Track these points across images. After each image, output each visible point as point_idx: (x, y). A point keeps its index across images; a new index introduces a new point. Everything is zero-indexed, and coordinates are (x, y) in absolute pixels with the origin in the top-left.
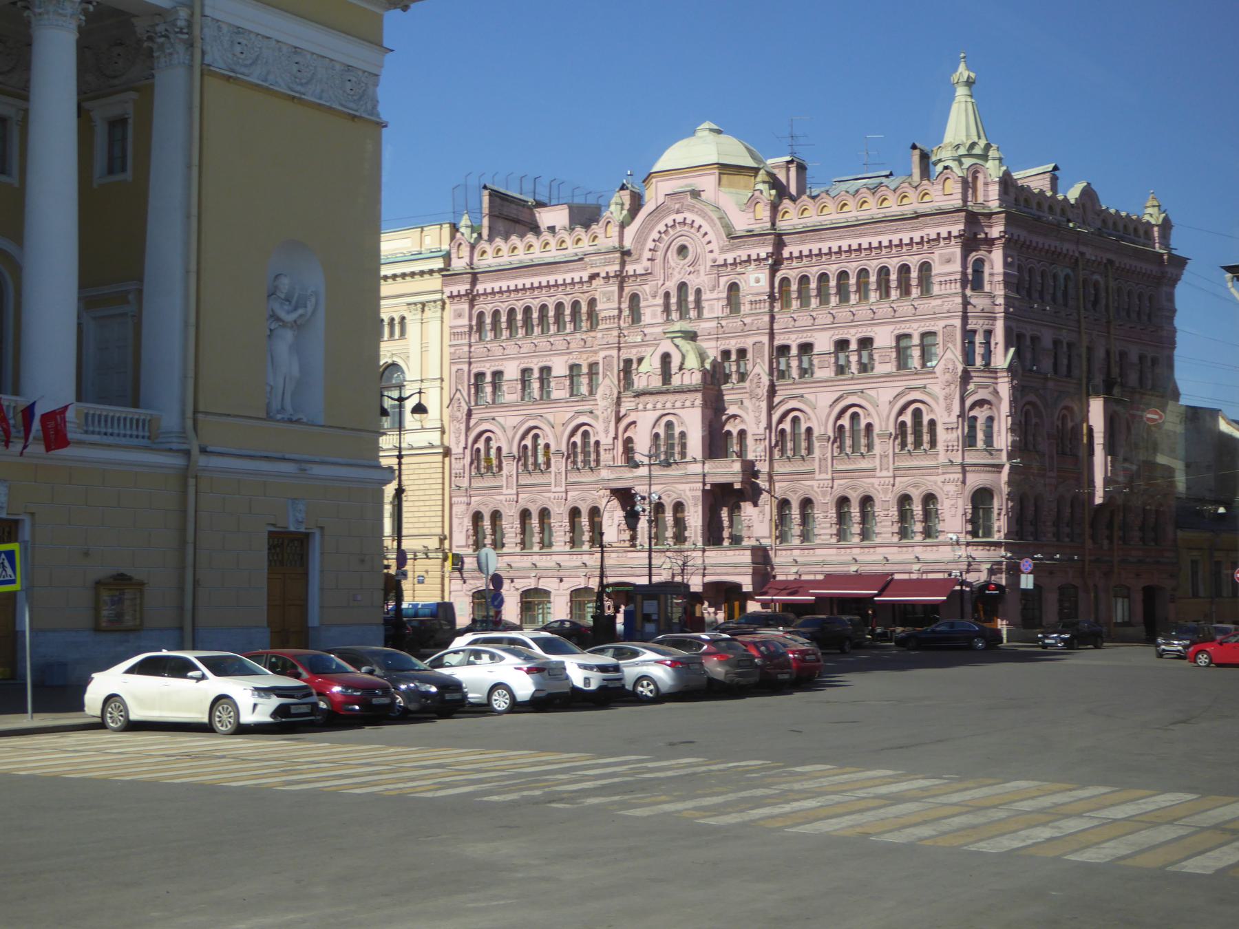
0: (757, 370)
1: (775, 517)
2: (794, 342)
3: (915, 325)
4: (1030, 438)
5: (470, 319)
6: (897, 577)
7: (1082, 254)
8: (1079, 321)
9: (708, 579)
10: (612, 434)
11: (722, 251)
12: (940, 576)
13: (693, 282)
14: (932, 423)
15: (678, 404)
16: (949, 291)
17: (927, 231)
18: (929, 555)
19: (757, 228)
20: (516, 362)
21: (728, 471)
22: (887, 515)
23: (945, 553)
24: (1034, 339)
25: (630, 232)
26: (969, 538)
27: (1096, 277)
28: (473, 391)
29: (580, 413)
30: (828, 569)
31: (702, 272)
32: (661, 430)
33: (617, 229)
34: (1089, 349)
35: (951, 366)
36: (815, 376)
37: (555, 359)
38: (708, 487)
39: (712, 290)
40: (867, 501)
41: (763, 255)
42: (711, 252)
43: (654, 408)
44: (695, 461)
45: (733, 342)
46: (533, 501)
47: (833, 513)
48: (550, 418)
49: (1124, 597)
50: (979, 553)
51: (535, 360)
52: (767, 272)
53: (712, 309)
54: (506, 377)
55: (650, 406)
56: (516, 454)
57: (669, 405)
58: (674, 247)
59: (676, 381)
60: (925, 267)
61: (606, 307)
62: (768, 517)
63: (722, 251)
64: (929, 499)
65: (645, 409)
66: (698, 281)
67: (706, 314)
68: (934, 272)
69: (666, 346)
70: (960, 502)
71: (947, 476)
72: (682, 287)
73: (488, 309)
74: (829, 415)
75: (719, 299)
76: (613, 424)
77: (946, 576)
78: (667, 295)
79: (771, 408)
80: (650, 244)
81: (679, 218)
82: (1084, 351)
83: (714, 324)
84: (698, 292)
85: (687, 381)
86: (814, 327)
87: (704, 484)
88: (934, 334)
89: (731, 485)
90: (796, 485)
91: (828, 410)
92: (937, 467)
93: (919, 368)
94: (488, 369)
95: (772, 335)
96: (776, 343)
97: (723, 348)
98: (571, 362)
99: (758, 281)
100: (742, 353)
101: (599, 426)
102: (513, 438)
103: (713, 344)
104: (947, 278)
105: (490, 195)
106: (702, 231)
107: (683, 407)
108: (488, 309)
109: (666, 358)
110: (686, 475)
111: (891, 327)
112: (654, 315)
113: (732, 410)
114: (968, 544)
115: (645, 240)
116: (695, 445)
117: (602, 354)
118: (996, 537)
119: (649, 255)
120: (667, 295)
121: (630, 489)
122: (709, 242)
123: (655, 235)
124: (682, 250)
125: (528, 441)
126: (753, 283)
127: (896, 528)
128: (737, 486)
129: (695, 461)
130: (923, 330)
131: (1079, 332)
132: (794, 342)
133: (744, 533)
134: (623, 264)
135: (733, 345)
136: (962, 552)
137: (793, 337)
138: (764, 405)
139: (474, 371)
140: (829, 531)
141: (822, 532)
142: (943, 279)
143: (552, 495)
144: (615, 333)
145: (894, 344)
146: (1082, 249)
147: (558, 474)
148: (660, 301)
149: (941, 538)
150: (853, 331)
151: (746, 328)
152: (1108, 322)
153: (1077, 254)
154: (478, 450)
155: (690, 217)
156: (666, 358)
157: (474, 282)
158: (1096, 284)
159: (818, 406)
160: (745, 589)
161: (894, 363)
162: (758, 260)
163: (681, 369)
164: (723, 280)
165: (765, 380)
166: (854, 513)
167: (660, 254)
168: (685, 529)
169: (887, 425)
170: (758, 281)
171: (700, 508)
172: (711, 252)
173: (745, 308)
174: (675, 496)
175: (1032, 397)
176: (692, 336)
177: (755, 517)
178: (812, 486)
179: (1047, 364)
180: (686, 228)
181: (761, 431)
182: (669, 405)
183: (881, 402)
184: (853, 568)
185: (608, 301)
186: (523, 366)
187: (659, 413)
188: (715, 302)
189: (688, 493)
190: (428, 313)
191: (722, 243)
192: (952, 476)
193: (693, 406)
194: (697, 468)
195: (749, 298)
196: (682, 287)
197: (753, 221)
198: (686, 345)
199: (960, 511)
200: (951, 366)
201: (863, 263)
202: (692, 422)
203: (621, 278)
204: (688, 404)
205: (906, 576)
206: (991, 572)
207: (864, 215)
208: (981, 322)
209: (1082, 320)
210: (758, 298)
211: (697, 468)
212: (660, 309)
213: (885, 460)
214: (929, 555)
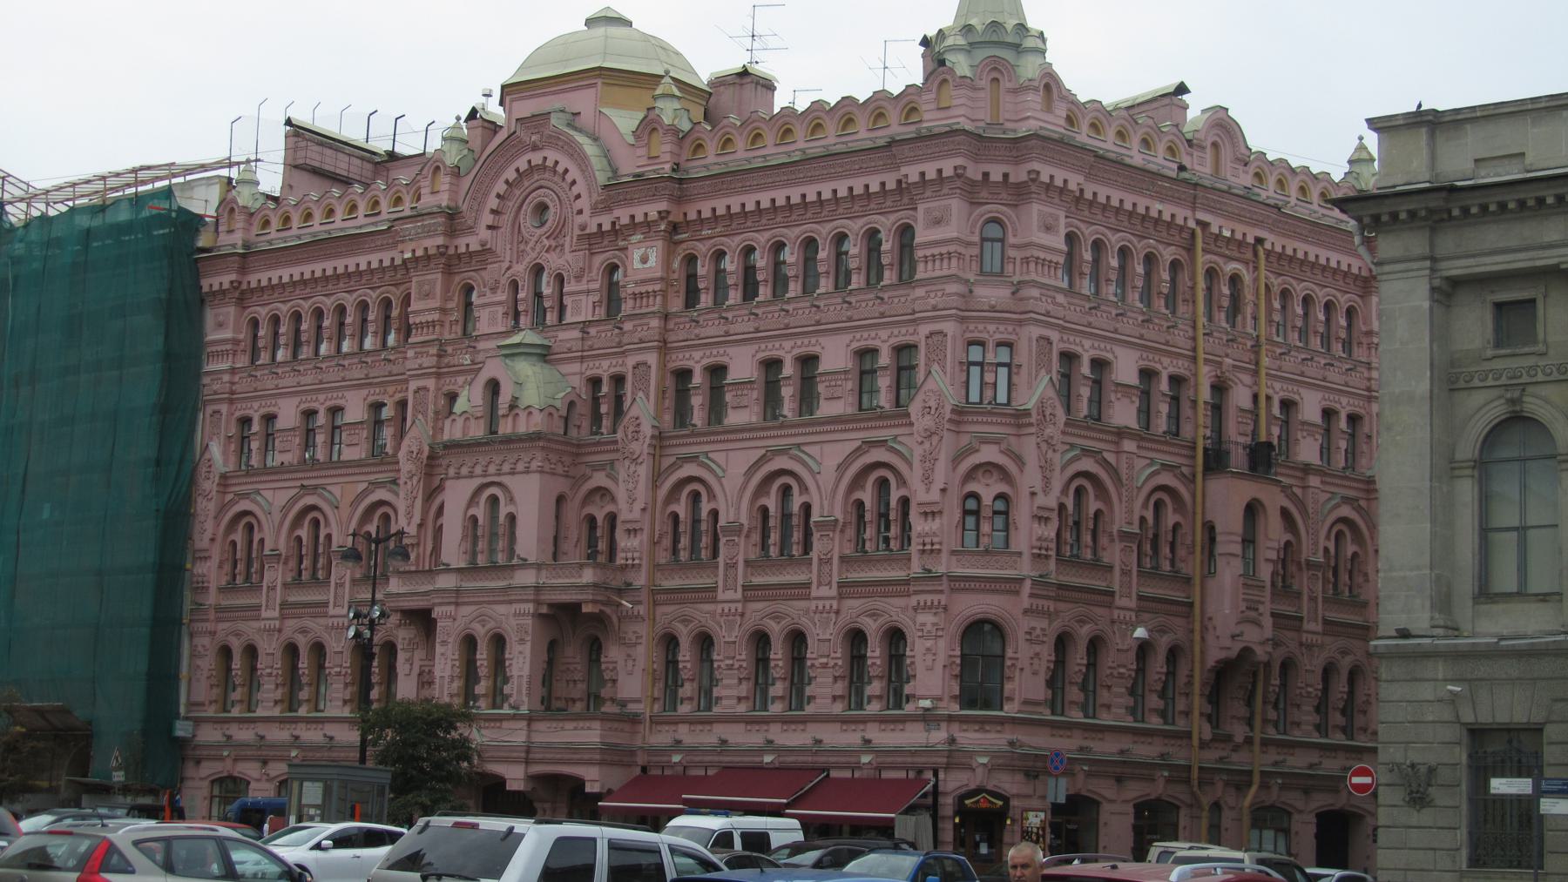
0: (633, 412)
1: (659, 666)
2: (697, 362)
3: (884, 334)
4: (1087, 538)
5: (237, 330)
6: (834, 774)
7: (1204, 225)
8: (1194, 339)
10: (417, 519)
11: (596, 210)
12: (901, 775)
13: (553, 262)
14: (905, 502)
15: (506, 468)
16: (938, 273)
17: (904, 170)
18: (886, 738)
19: (650, 171)
21: (579, 581)
22: (825, 666)
23: (913, 737)
24: (1099, 365)
25: (466, 183)
26: (955, 709)
27: (1231, 267)
28: (233, 447)
29: (376, 485)
30: (726, 759)
32: (480, 511)
33: (448, 179)
34: (1220, 388)
35: (933, 404)
36: (726, 422)
38: (544, 610)
39: (578, 278)
40: (797, 639)
41: (653, 215)
42: (580, 212)
43: (471, 476)
44: (524, 564)
45: (605, 364)
46: (304, 631)
47: (744, 657)
48: (336, 490)
49: (1278, 830)
50: (969, 738)
51: (322, 397)
52: (660, 244)
53: (577, 311)
54: (281, 424)
55: (464, 471)
56: (283, 552)
57: (492, 469)
58: (528, 208)
59: (505, 428)
60: (906, 231)
61: (422, 309)
62: (641, 663)
64: (895, 637)
65: (458, 477)
66: (561, 261)
67: (569, 318)
68: (917, 240)
69: (492, 369)
70: (942, 643)
71: (922, 598)
72: (538, 270)
73: (263, 313)
74: (744, 488)
75: (588, 292)
76: (419, 503)
77: (912, 775)
78: (514, 285)
79: (656, 479)
80: (493, 202)
81: (536, 158)
82: (1205, 394)
83: (576, 334)
84: (560, 279)
85: (522, 429)
86: (727, 341)
87: (538, 603)
88: (912, 347)
90: (688, 610)
91: (741, 479)
92: (907, 582)
93: (887, 406)
94: (256, 412)
95: (664, 347)
96: (672, 365)
97: (589, 373)
98: (371, 399)
99: (644, 260)
100: (619, 380)
101: (402, 506)
102: (281, 524)
103: (576, 367)
104: (936, 251)
105: (297, 135)
106: (569, 178)
107: (513, 473)
108: (263, 313)
109: (494, 387)
110: (510, 587)
111: (846, 338)
112: (492, 321)
113: (599, 479)
114: (951, 719)
115: (486, 195)
116: (529, 540)
117: (413, 385)
118: (1010, 710)
119: (488, 219)
120: (514, 285)
122: (578, 197)
123: (500, 187)
124: (542, 208)
125: (304, 533)
126: (637, 265)
127: (840, 688)
128: (586, 609)
129: (524, 564)
130: (894, 341)
131: (1194, 359)
132: (697, 362)
133: (605, 692)
135: (605, 369)
136: (939, 736)
137: (697, 355)
138: (643, 471)
139: (238, 414)
140: (735, 693)
141: (724, 693)
142: (928, 252)
143: (330, 622)
144: (433, 350)
145: (850, 366)
146: (1201, 216)
147: (340, 585)
148: (502, 296)
149: (909, 708)
150: (788, 344)
151: (625, 339)
152: (1256, 347)
153: (1191, 224)
154: (234, 543)
155: (552, 155)
156: (494, 387)
157: (243, 270)
158: (1235, 280)
159: (731, 475)
161: (852, 399)
162: (648, 225)
163: (512, 407)
164: (598, 260)
165: (647, 430)
166: (778, 659)
167: (506, 219)
168: (506, 680)
169: (832, 506)
170: (644, 260)
171: (527, 648)
172: (580, 212)
173: (627, 307)
174: (492, 624)
175: (1087, 465)
176: (545, 355)
177: (621, 664)
178: (713, 614)
179: (1123, 413)
180: (547, 175)
181: (636, 514)
183: (825, 469)
184: (768, 759)
185: (428, 300)
186: (304, 406)
187: (477, 482)
188: (583, 297)
191: (595, 197)
192: (929, 598)
193: (527, 471)
195: (631, 288)
196: (538, 270)
197: (644, 161)
198: (527, 369)
199: (941, 659)
200: (933, 404)
201: (808, 229)
202: (528, 498)
203: (450, 262)
204: (520, 467)
205: (848, 774)
206: (991, 769)
207: (815, 148)
208: (991, 328)
209: (1201, 338)
211: (526, 578)
212: (501, 310)
213: (826, 569)
214: (886, 738)
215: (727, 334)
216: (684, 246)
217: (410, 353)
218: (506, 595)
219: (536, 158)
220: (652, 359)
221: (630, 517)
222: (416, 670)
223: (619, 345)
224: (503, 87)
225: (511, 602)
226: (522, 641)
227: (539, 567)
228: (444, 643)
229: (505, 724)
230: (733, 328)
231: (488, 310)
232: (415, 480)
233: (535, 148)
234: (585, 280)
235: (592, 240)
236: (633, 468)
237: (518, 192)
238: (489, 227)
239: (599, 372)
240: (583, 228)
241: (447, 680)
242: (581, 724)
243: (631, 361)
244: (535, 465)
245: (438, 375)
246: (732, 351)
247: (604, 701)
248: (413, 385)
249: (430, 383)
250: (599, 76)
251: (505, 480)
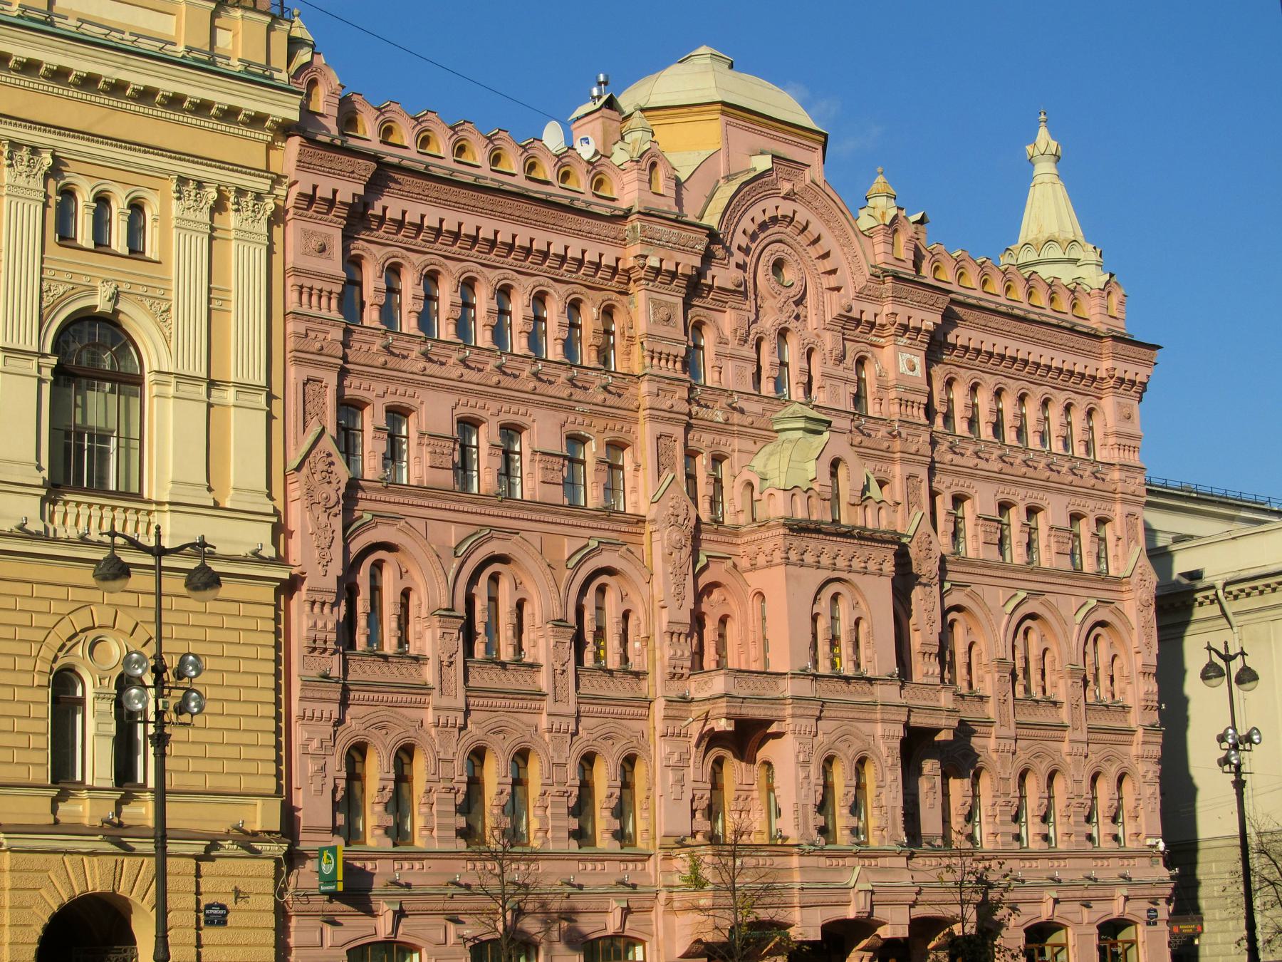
9: (919, 912)
15: (857, 564)
20: (452, 399)
55: (809, 558)
57: (841, 563)
86: (971, 474)
107: (865, 572)
124: (778, 266)
134: (708, 258)
182: (841, 563)
186: (462, 411)
187: (824, 575)
190: (231, 219)
194: (890, 693)
204: (872, 566)
210: (911, 397)
219: (786, 208)
246: (974, 483)
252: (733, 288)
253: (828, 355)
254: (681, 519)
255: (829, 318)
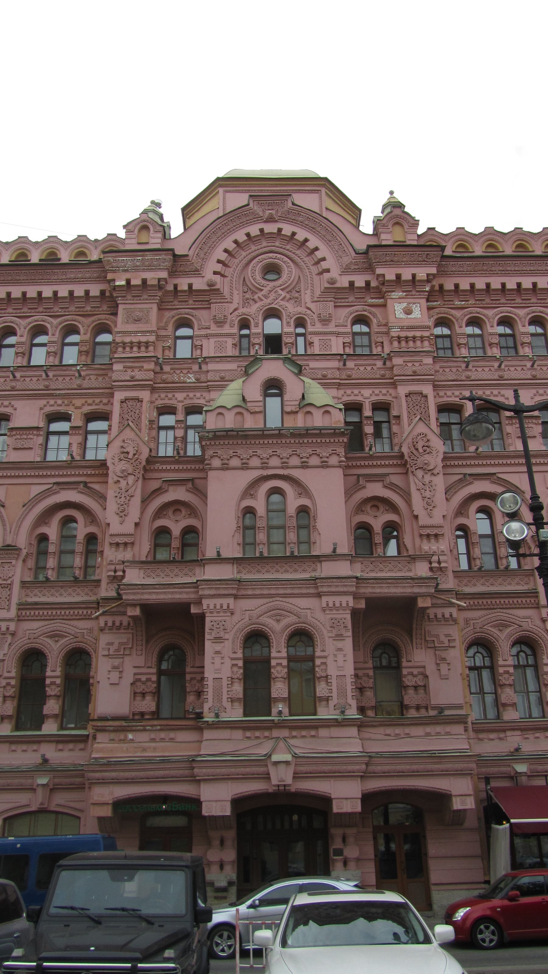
31: (307, 297)
37: (17, 404)
38: (362, 605)
39: (325, 321)
43: (245, 467)
45: (367, 392)
58: (257, 266)
63: (346, 270)
65: (225, 467)
75: (338, 334)
76: (137, 501)
83: (335, 364)
89: (412, 600)
99: (408, 312)
121: (186, 606)
123: (241, 236)
135: (367, 396)
160: (457, 804)
170: (408, 312)
171: (348, 645)
188: (333, 338)
189: (319, 615)
191: (346, 260)
193: (324, 465)
194: (343, 569)
215: (501, 378)
216: (436, 310)
217: (116, 367)
218: (316, 587)
220: (428, 389)
221: (429, 522)
222: (129, 678)
223: (383, 377)
224: (218, 179)
225: (319, 595)
226: (339, 637)
227: (352, 558)
228: (218, 640)
229: (323, 732)
230: (506, 375)
231: (212, 340)
232: (131, 479)
233: (271, 220)
234: (333, 324)
235: (336, 294)
236: (428, 478)
237: (264, 244)
238: (215, 273)
239: (359, 398)
240: (332, 282)
241: (225, 682)
242: (439, 729)
243: (403, 390)
244: (334, 460)
245: (153, 390)
247: (407, 707)
248: (119, 396)
249: (145, 395)
250: (323, 186)
251: (296, 473)
252: (207, 288)
253: (316, 319)
254: (130, 456)
255: (318, 293)
